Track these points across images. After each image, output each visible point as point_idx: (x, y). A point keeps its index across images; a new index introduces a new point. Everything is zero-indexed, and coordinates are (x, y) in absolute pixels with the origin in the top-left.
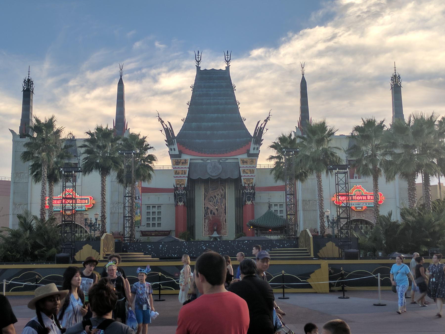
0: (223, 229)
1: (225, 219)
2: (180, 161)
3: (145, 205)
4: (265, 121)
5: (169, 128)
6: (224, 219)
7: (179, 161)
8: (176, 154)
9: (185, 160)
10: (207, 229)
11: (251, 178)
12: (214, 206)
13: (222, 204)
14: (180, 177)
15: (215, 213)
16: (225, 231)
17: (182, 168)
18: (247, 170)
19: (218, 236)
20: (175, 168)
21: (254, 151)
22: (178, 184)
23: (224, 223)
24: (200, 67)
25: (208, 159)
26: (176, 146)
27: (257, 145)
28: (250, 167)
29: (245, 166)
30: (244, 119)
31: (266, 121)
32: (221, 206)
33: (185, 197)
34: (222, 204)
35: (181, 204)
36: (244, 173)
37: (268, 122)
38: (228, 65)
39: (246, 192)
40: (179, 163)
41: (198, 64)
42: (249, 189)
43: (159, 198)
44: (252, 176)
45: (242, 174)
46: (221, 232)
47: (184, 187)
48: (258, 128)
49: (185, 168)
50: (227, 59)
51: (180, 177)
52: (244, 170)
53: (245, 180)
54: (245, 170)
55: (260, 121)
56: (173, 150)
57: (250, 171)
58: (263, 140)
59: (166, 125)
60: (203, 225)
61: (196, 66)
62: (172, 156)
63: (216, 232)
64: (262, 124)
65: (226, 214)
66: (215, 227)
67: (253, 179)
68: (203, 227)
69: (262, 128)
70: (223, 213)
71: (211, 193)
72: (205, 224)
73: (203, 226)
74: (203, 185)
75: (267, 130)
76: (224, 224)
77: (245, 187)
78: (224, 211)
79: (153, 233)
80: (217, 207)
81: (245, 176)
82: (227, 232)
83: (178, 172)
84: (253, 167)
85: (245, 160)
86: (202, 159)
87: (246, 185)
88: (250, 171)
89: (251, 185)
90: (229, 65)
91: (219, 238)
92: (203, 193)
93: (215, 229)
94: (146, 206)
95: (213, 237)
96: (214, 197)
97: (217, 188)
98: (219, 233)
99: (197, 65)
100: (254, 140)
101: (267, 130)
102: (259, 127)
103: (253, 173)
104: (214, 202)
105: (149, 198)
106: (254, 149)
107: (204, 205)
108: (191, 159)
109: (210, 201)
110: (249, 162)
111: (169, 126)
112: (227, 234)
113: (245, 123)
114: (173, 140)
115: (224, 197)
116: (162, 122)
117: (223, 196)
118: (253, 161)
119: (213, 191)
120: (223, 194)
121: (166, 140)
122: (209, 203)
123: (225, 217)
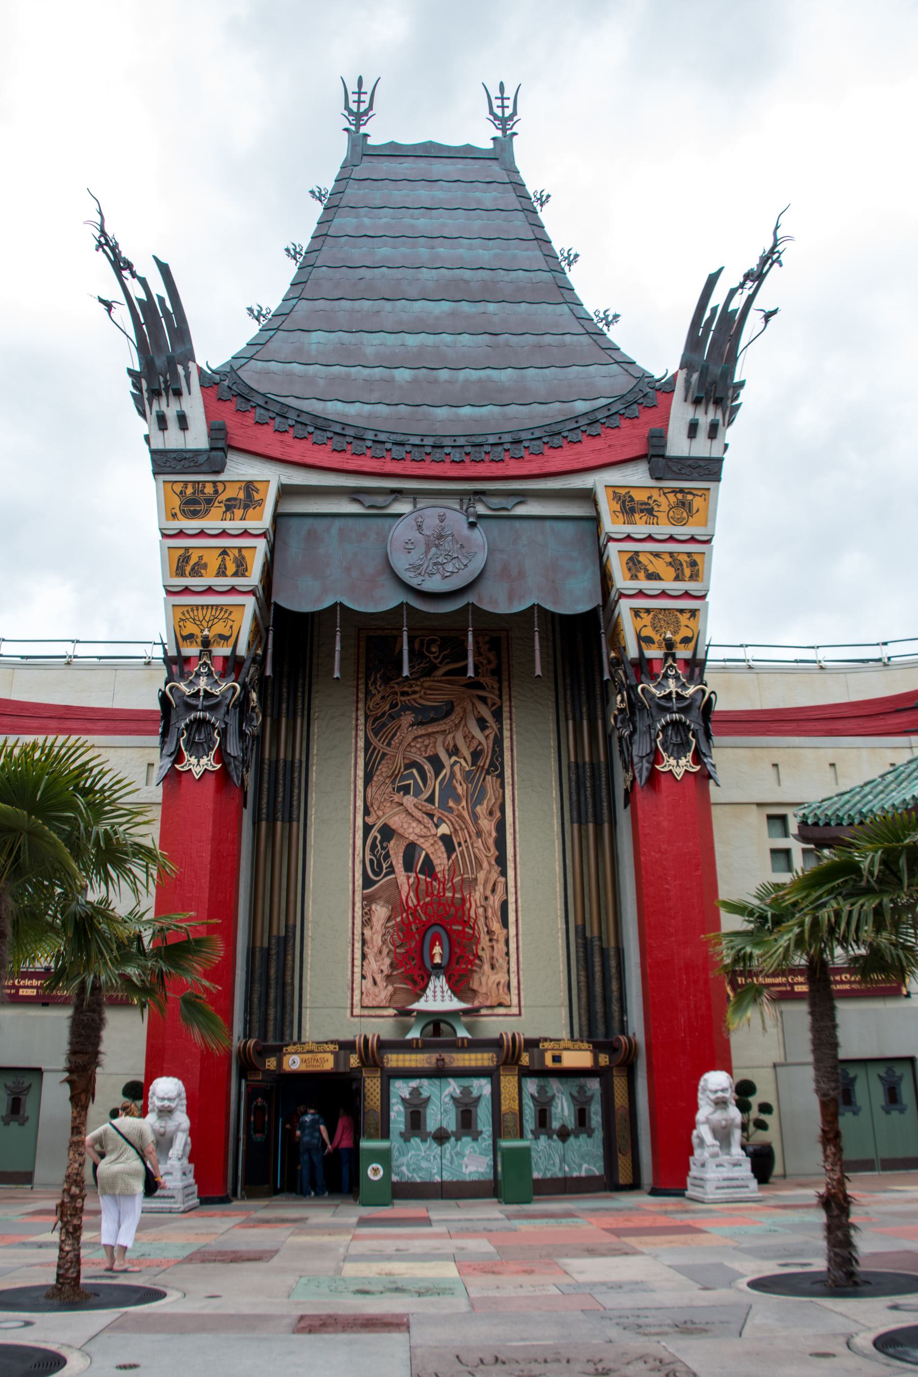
0: (486, 967)
1: (497, 905)
2: (216, 492)
4: (747, 277)
5: (161, 300)
6: (495, 901)
7: (209, 489)
8: (192, 446)
9: (249, 487)
10: (379, 965)
11: (682, 611)
12: (431, 816)
13: (481, 810)
14: (210, 590)
15: (436, 862)
16: (502, 977)
17: (224, 534)
18: (657, 555)
19: (455, 1004)
20: (181, 534)
21: (695, 442)
22: (190, 637)
23: (496, 926)
24: (366, 136)
27: (711, 408)
28: (672, 539)
29: (640, 529)
30: (607, 317)
31: (756, 276)
32: (475, 817)
33: (233, 721)
34: (481, 810)
36: (634, 577)
37: (774, 274)
38: (504, 131)
39: (658, 693)
40: (209, 501)
41: (358, 126)
42: (677, 678)
44: (687, 595)
45: (621, 581)
46: (475, 985)
47: (226, 658)
48: (707, 314)
49: (245, 534)
50: (499, 112)
51: (210, 590)
52: (637, 553)
53: (647, 619)
54: (642, 558)
55: (721, 270)
56: (173, 423)
57: (674, 561)
58: (741, 384)
59: (143, 282)
60: (358, 937)
61: (346, 130)
63: (443, 979)
64: (732, 293)
65: (504, 873)
66: (437, 950)
67: (693, 613)
68: (358, 955)
69: (736, 311)
70: (485, 865)
71: (409, 738)
72: (368, 933)
73: (358, 945)
74: (361, 696)
75: (767, 321)
76: (490, 932)
77: (643, 666)
78: (494, 852)
79: (27, 982)
80: (444, 829)
81: (641, 594)
82: (514, 983)
83: (193, 560)
84: (693, 540)
85: (636, 498)
87: (654, 653)
88: (674, 561)
89: (683, 653)
90: (509, 132)
91: (469, 1028)
92: (361, 744)
93: (437, 960)
95: (422, 1014)
96: (427, 767)
97: (448, 713)
98: (459, 987)
99: (353, 128)
100: (688, 381)
101: (767, 321)
102: (714, 310)
103: (694, 577)
104: (426, 795)
106: (693, 430)
107: (367, 812)
108: (285, 492)
109: (406, 790)
110: (664, 507)
111: (158, 288)
112: (515, 1001)
113: (614, 334)
114: (180, 368)
115: (492, 764)
116: (120, 265)
117: (485, 761)
119: (421, 731)
120: (487, 745)
121: (137, 368)
122: (396, 798)
123: (500, 888)
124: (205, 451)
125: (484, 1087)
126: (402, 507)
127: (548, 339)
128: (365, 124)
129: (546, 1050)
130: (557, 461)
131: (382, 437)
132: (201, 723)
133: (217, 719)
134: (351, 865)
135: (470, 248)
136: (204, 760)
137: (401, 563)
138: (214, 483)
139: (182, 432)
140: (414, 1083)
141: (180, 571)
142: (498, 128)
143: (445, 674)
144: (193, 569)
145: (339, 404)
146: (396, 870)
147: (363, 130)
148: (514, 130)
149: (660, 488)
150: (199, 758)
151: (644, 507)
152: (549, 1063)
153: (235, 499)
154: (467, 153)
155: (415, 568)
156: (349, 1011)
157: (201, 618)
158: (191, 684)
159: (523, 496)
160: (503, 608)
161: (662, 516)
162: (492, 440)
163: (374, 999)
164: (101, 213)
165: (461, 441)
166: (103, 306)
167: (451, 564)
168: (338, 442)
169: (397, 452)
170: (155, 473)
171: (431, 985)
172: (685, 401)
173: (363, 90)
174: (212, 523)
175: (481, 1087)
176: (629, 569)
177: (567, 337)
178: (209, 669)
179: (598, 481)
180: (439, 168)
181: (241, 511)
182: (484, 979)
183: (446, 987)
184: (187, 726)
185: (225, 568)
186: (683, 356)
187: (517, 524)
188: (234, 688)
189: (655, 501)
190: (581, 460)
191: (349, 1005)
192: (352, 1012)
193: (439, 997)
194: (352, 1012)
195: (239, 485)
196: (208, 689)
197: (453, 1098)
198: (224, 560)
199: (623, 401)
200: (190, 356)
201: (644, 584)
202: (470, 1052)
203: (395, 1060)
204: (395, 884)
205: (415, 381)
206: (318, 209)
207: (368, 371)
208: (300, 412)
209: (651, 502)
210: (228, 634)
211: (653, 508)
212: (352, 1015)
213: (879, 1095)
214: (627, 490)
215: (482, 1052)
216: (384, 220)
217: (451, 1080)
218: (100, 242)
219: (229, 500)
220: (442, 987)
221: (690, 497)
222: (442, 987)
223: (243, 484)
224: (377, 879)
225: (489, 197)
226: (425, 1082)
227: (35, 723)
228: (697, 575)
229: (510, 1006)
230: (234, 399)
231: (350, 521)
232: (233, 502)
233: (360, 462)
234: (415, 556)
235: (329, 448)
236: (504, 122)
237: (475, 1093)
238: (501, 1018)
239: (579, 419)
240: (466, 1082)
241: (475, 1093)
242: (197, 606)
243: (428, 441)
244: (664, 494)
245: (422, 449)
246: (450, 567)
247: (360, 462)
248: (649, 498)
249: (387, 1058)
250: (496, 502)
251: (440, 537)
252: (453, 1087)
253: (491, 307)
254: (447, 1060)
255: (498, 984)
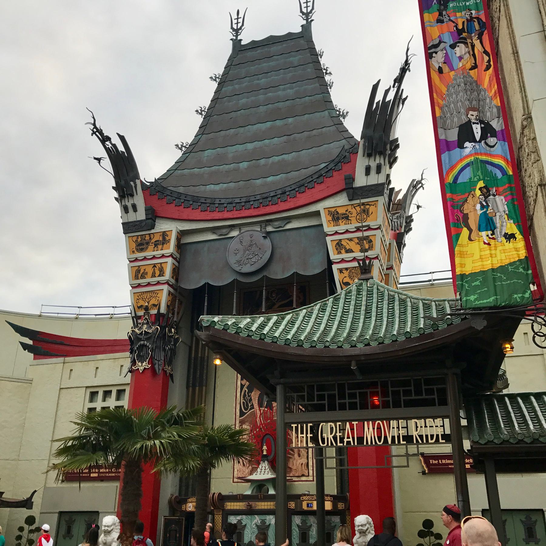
0: (296, 455)
2: (150, 239)
3: (87, 387)
7: (147, 238)
8: (139, 219)
9: (164, 234)
14: (149, 284)
17: (154, 257)
18: (351, 240)
20: (136, 260)
22: (140, 307)
24: (241, 40)
25: (232, 227)
26: (139, 200)
27: (378, 157)
29: (342, 227)
31: (399, 80)
35: (142, 366)
36: (340, 253)
38: (307, 20)
40: (148, 243)
41: (237, 36)
43: (122, 366)
45: (333, 256)
49: (163, 256)
51: (149, 284)
52: (340, 240)
53: (346, 273)
61: (231, 39)
62: (128, 228)
63: (266, 462)
64: (387, 92)
81: (343, 261)
83: (142, 271)
86: (213, 230)
90: (309, 20)
93: (265, 453)
94: (89, 391)
99: (234, 38)
105: (97, 368)
106: (368, 171)
110: (354, 214)
111: (121, 148)
116: (104, 139)
118: (368, 210)
124: (144, 220)
125: (271, 520)
126: (235, 233)
127: (315, 132)
128: (240, 34)
129: (303, 501)
130: (302, 199)
131: (223, 201)
132: (144, 345)
133: (150, 344)
134: (234, 405)
135: (284, 90)
136: (144, 364)
137: (232, 260)
138: (149, 234)
139: (134, 213)
140: (239, 518)
141: (136, 277)
142: (304, 19)
143: (278, 308)
144: (142, 276)
145: (212, 186)
146: (255, 407)
147: (239, 38)
148: (312, 19)
149: (352, 205)
150: (142, 363)
151: (344, 216)
152: (305, 507)
153: (158, 241)
154: (290, 36)
155: (239, 262)
156: (232, 480)
157: (145, 298)
158: (140, 328)
159: (289, 219)
160: (279, 277)
161: (353, 220)
162: (272, 194)
163: (243, 474)
164: (94, 118)
165: (258, 197)
166: (96, 161)
167: (254, 258)
168: (204, 207)
169: (230, 207)
170: (125, 233)
171: (260, 466)
172: (364, 156)
173: (239, 17)
174: (149, 253)
175: (270, 520)
176: (337, 249)
177: (324, 129)
178: (148, 321)
179: (320, 207)
180: (274, 49)
181: (161, 246)
182: (295, 462)
183: (267, 468)
184: (137, 348)
185: (155, 273)
186: (362, 132)
187: (288, 233)
188: (158, 328)
189: (349, 212)
190: (314, 197)
191: (232, 477)
192: (233, 480)
193: (263, 473)
194: (233, 480)
195: (160, 234)
196: (146, 330)
197: (257, 525)
198: (154, 269)
199: (334, 162)
200: (137, 176)
201: (345, 256)
202: (265, 502)
203: (230, 506)
204: (254, 414)
205: (249, 167)
206: (215, 85)
207: (228, 166)
208: (186, 195)
209: (347, 213)
210: (156, 304)
211: (348, 216)
212: (233, 482)
213: (521, 533)
214: (335, 209)
215: (271, 502)
216: (245, 84)
217: (256, 516)
218: (93, 131)
219: (156, 241)
220: (265, 467)
221: (367, 207)
222: (265, 467)
223: (162, 233)
224: (246, 412)
225: (295, 59)
226: (244, 517)
227: (102, 349)
228: (372, 247)
229: (308, 476)
230: (157, 193)
231: (213, 243)
232: (157, 242)
233: (213, 215)
234: (238, 257)
235: (200, 210)
236: (307, 15)
237: (267, 523)
238: (304, 483)
239: (313, 176)
240: (263, 517)
241: (267, 523)
242: (144, 292)
243: (243, 200)
244: (354, 207)
245: (240, 204)
246: (253, 260)
247: (213, 215)
248: (346, 211)
249: (226, 505)
250: (277, 224)
251: (251, 245)
252: (257, 519)
253: (290, 120)
254: (253, 506)
255: (302, 464)
